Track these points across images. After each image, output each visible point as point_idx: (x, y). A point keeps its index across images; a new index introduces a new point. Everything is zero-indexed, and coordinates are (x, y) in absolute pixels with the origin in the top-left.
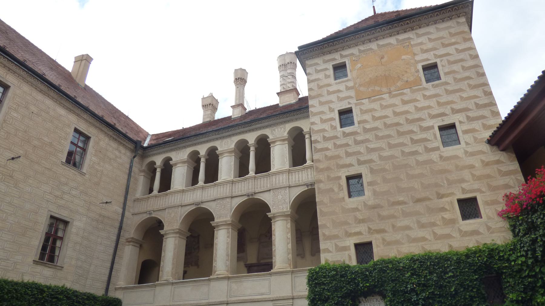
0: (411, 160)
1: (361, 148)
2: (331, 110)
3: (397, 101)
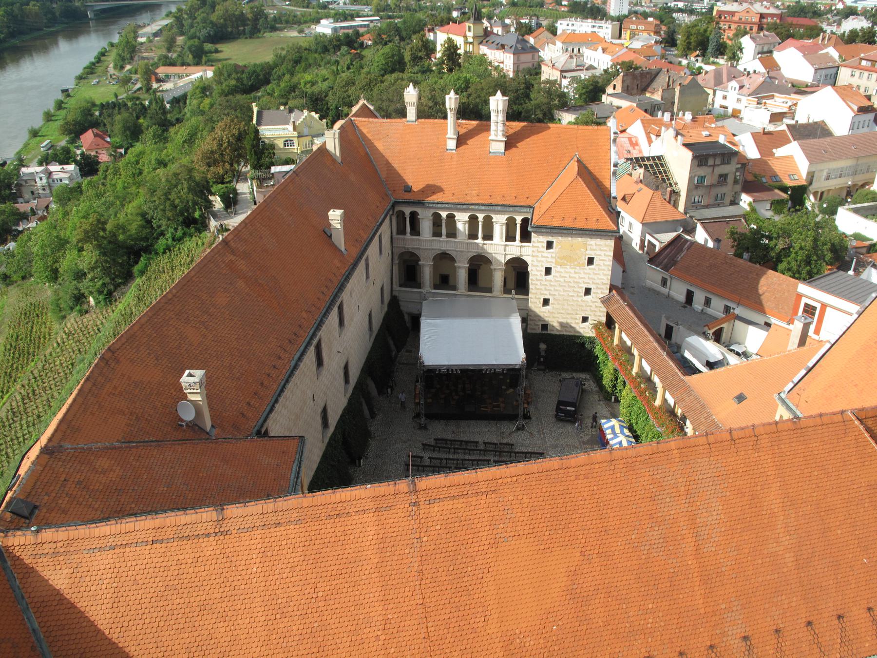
0: (570, 298)
1: (552, 288)
2: (542, 266)
3: (572, 271)
